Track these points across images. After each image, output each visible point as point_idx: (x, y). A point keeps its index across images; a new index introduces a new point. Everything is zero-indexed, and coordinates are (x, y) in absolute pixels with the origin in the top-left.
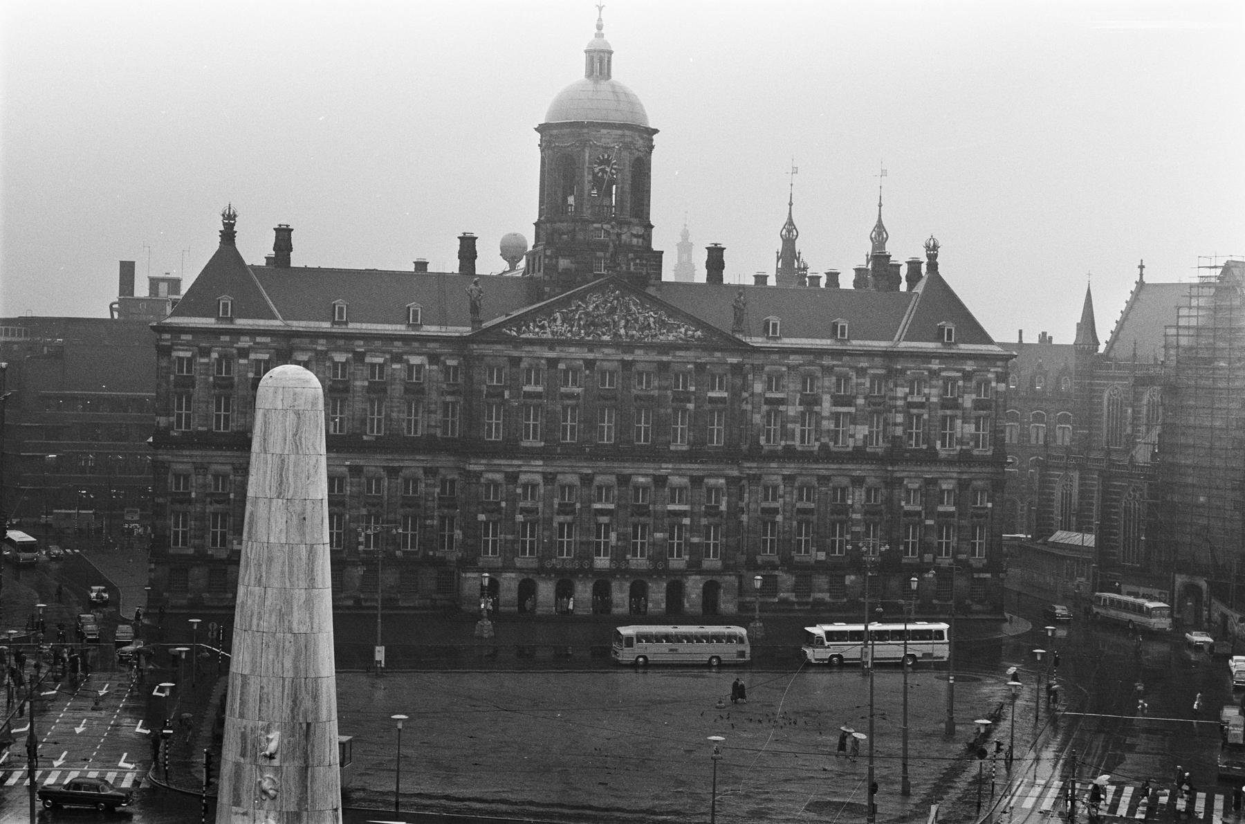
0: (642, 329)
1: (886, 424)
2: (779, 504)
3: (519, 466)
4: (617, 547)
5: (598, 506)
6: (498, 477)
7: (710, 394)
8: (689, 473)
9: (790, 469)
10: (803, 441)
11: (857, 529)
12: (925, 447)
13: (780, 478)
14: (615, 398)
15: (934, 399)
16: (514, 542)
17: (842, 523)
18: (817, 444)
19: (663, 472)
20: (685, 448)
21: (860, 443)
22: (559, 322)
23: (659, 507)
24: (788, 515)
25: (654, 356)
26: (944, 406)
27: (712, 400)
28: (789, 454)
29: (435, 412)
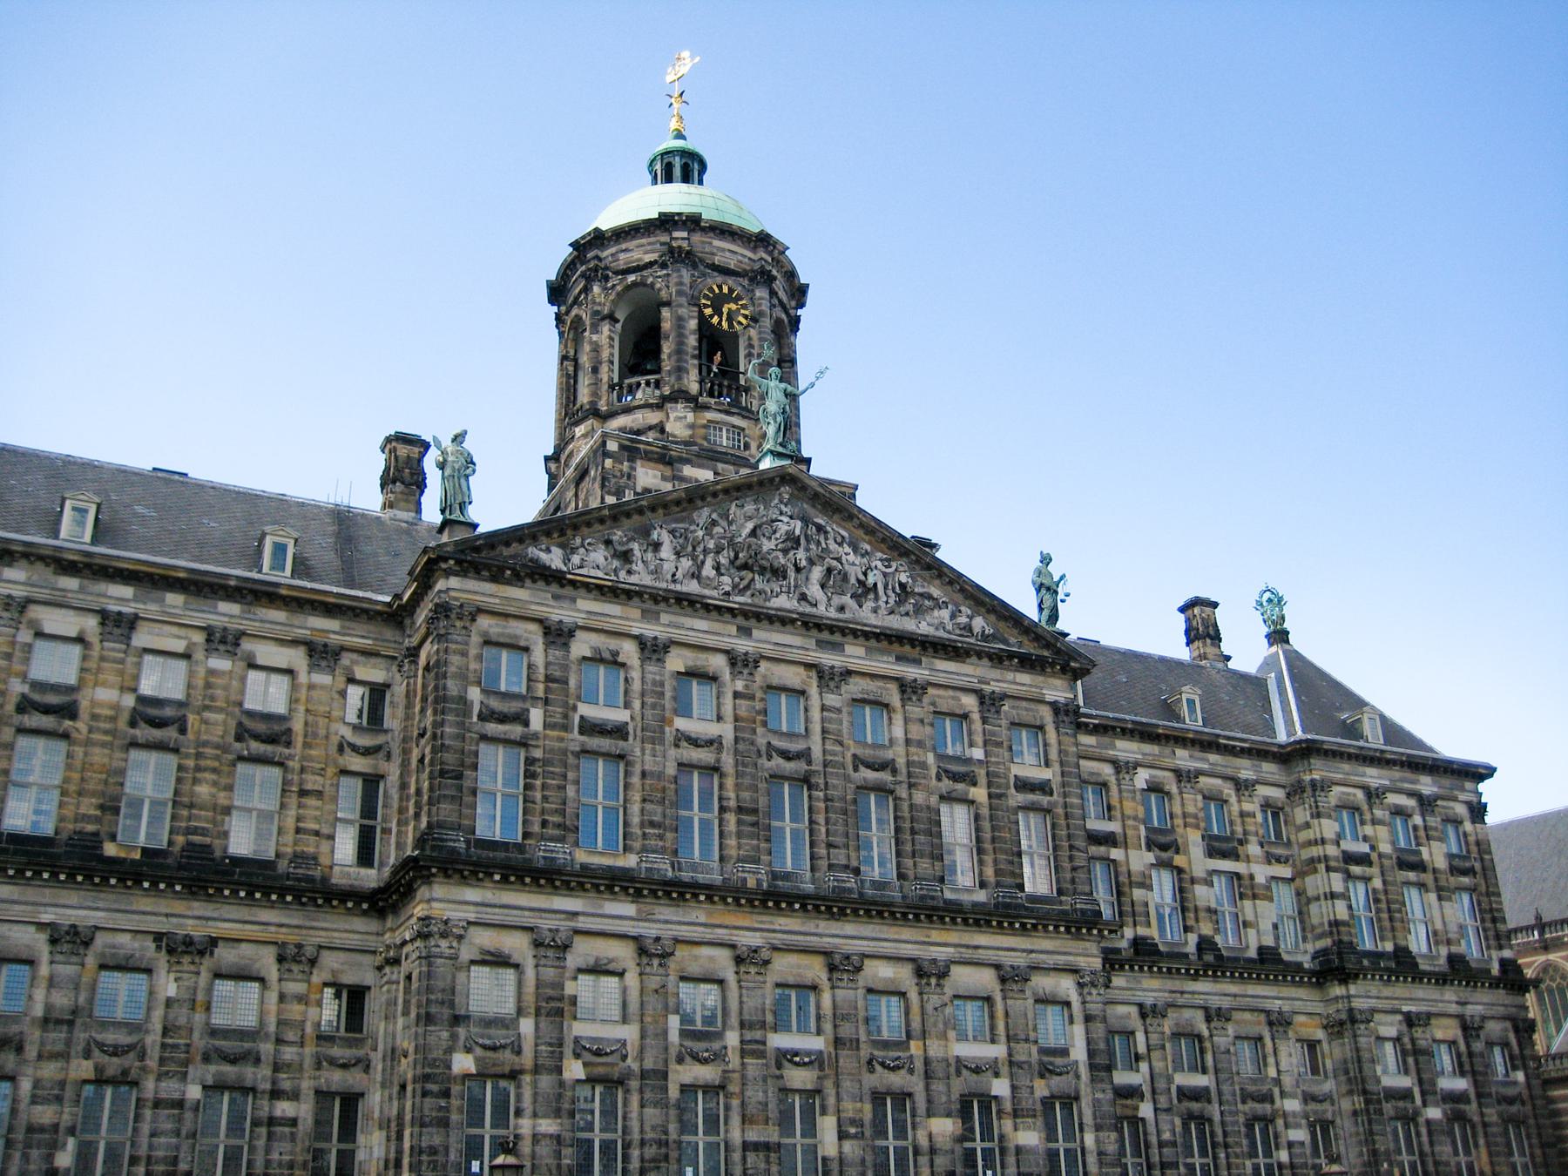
0: (859, 598)
1: (1303, 900)
3: (576, 914)
4: (841, 1160)
5: (778, 1041)
6: (516, 945)
7: (1016, 770)
9: (1152, 988)
10: (1161, 929)
11: (1299, 1135)
12: (1389, 947)
13: (1134, 1010)
14: (805, 755)
15: (1385, 848)
16: (558, 1139)
17: (1267, 1121)
18: (1192, 939)
19: (941, 953)
20: (981, 896)
21: (1269, 941)
22: (666, 552)
23: (935, 1049)
24: (1163, 1102)
25: (886, 664)
26: (1403, 865)
27: (1024, 785)
28: (1145, 954)
29: (319, 794)
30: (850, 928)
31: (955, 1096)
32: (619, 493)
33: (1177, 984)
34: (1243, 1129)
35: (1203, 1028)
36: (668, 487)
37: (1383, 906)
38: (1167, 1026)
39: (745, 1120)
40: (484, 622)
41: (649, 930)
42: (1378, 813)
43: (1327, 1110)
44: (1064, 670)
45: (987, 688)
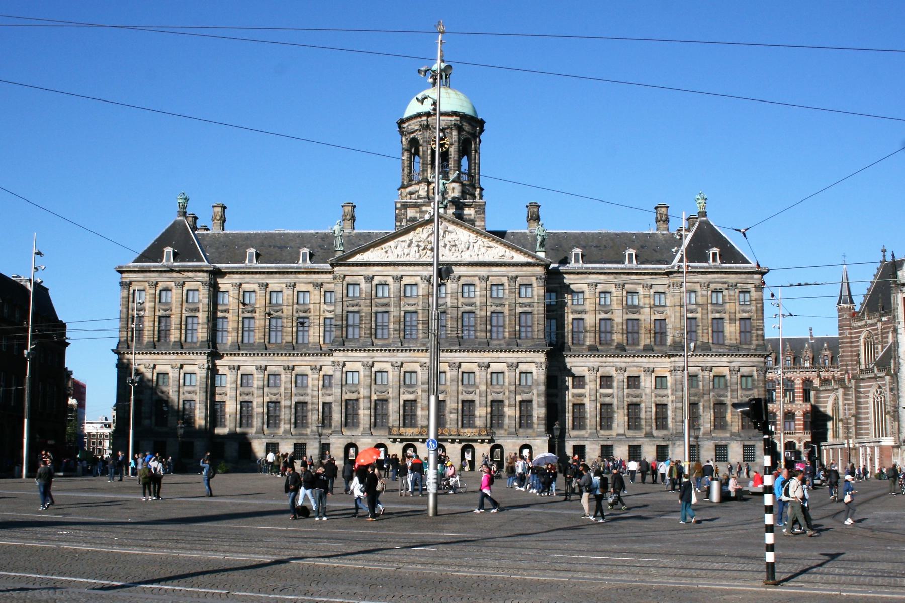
2: (586, 391)
6: (359, 367)
8: (504, 360)
19: (486, 361)
24: (593, 398)
30: (457, 354)
31: (489, 401)
32: (401, 221)
33: (604, 359)
34: (626, 407)
35: (613, 373)
36: (418, 215)
37: (700, 327)
38: (599, 374)
39: (422, 409)
40: (347, 278)
41: (393, 360)
42: (705, 293)
43: (664, 400)
44: (538, 265)
45: (510, 275)
